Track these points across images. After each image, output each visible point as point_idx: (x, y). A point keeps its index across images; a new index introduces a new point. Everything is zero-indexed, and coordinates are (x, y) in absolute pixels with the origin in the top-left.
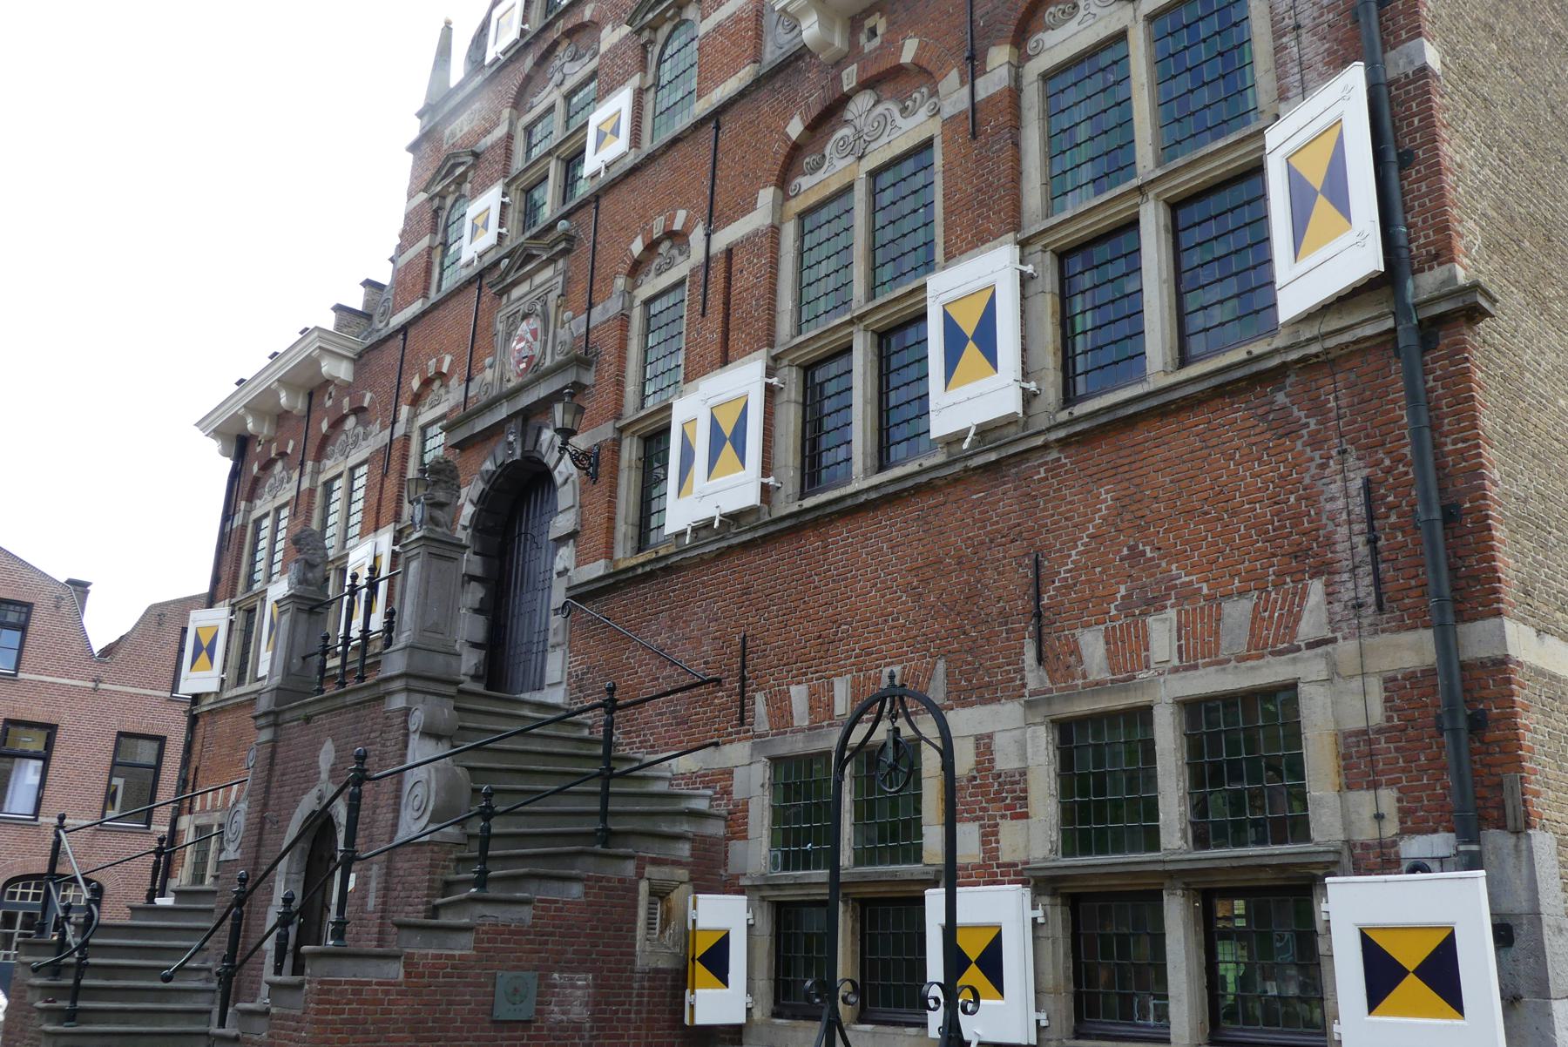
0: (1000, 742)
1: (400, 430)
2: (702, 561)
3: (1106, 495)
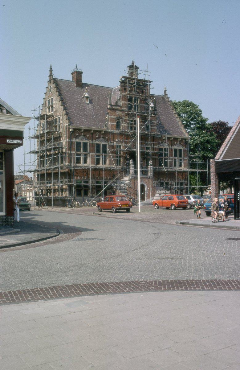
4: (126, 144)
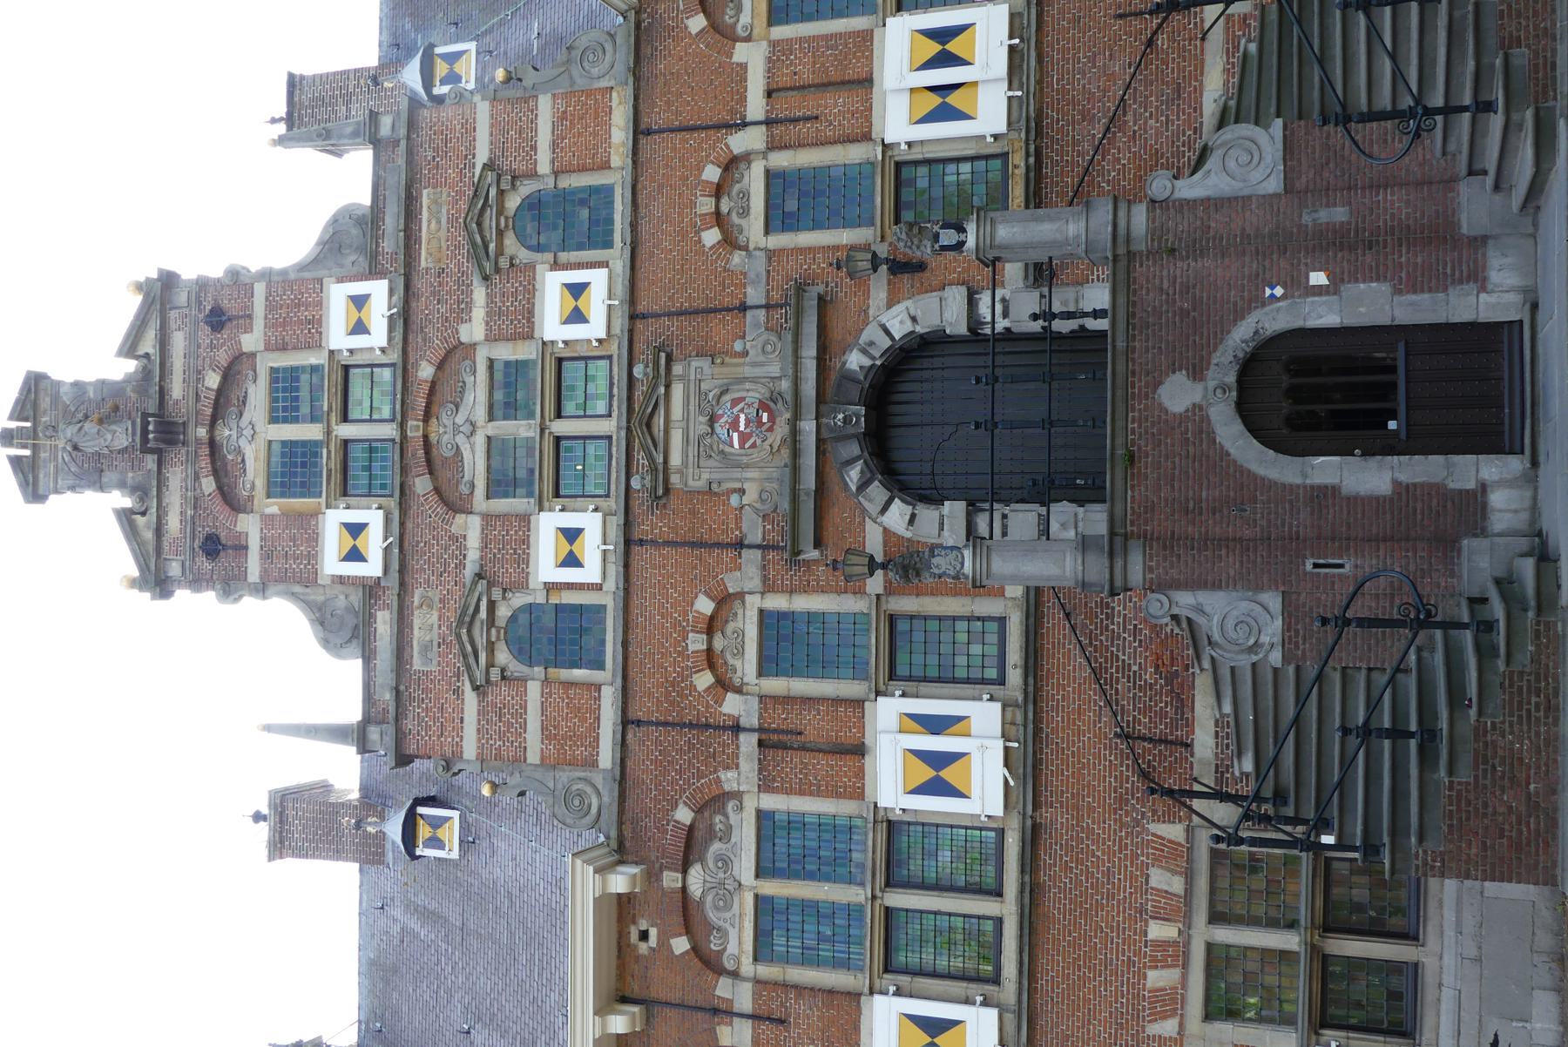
2: (1039, 82)
4: (740, 545)
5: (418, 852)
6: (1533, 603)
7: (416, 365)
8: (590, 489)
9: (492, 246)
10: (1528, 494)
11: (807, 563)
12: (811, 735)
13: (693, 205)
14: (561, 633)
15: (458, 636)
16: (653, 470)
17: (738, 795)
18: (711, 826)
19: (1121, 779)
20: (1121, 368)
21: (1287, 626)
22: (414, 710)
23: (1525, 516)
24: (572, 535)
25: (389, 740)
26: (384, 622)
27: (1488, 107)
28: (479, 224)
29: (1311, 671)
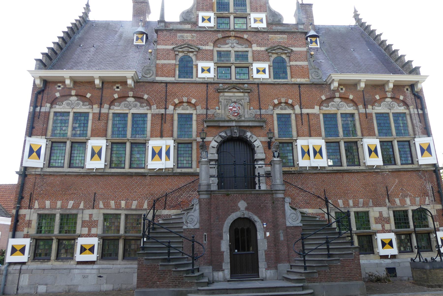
0: (383, 213)
1: (168, 112)
2: (310, 173)
3: (397, 181)
4: (207, 109)
5: (135, 35)
6: (198, 281)
7: (247, 34)
8: (219, 75)
9: (274, 51)
10: (222, 280)
11: (203, 124)
12: (165, 125)
13: (283, 97)
14: (186, 68)
15: (185, 44)
16: (224, 89)
17: (151, 109)
18: (143, 103)
19: (157, 194)
20: (248, 192)
21: (192, 229)
22: (168, 34)
23: (217, 279)
24: (209, 70)
25: (161, 28)
26: (188, 27)
27: (305, 269)
28: (279, 48)
29: (182, 235)
